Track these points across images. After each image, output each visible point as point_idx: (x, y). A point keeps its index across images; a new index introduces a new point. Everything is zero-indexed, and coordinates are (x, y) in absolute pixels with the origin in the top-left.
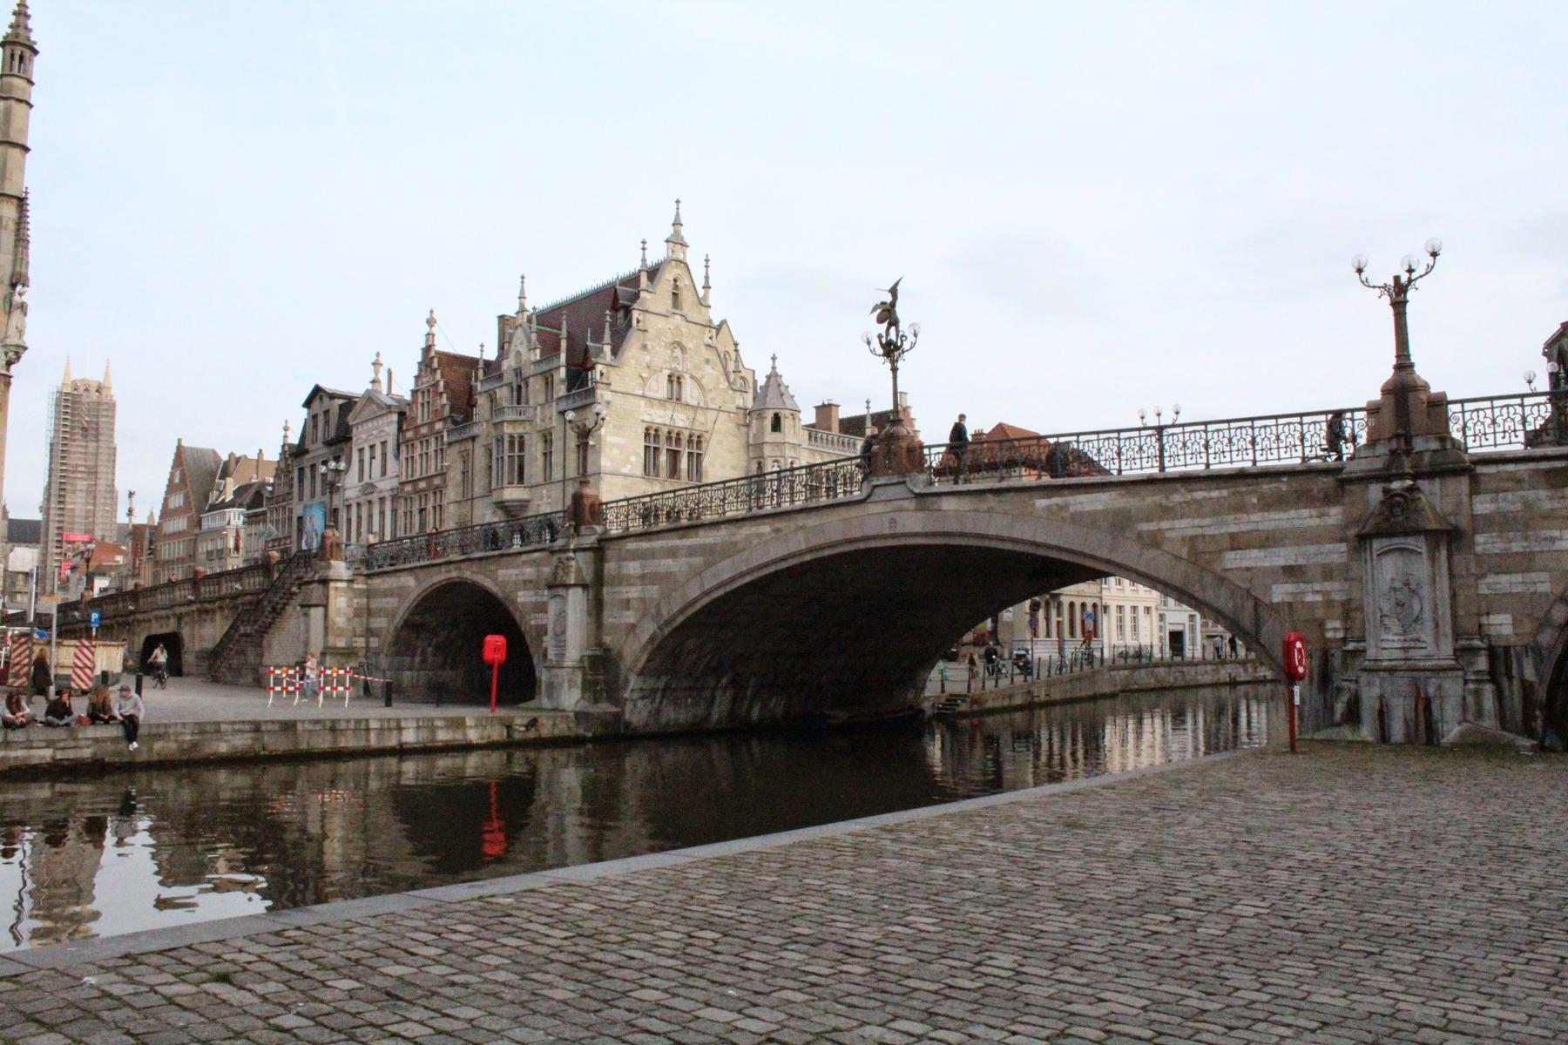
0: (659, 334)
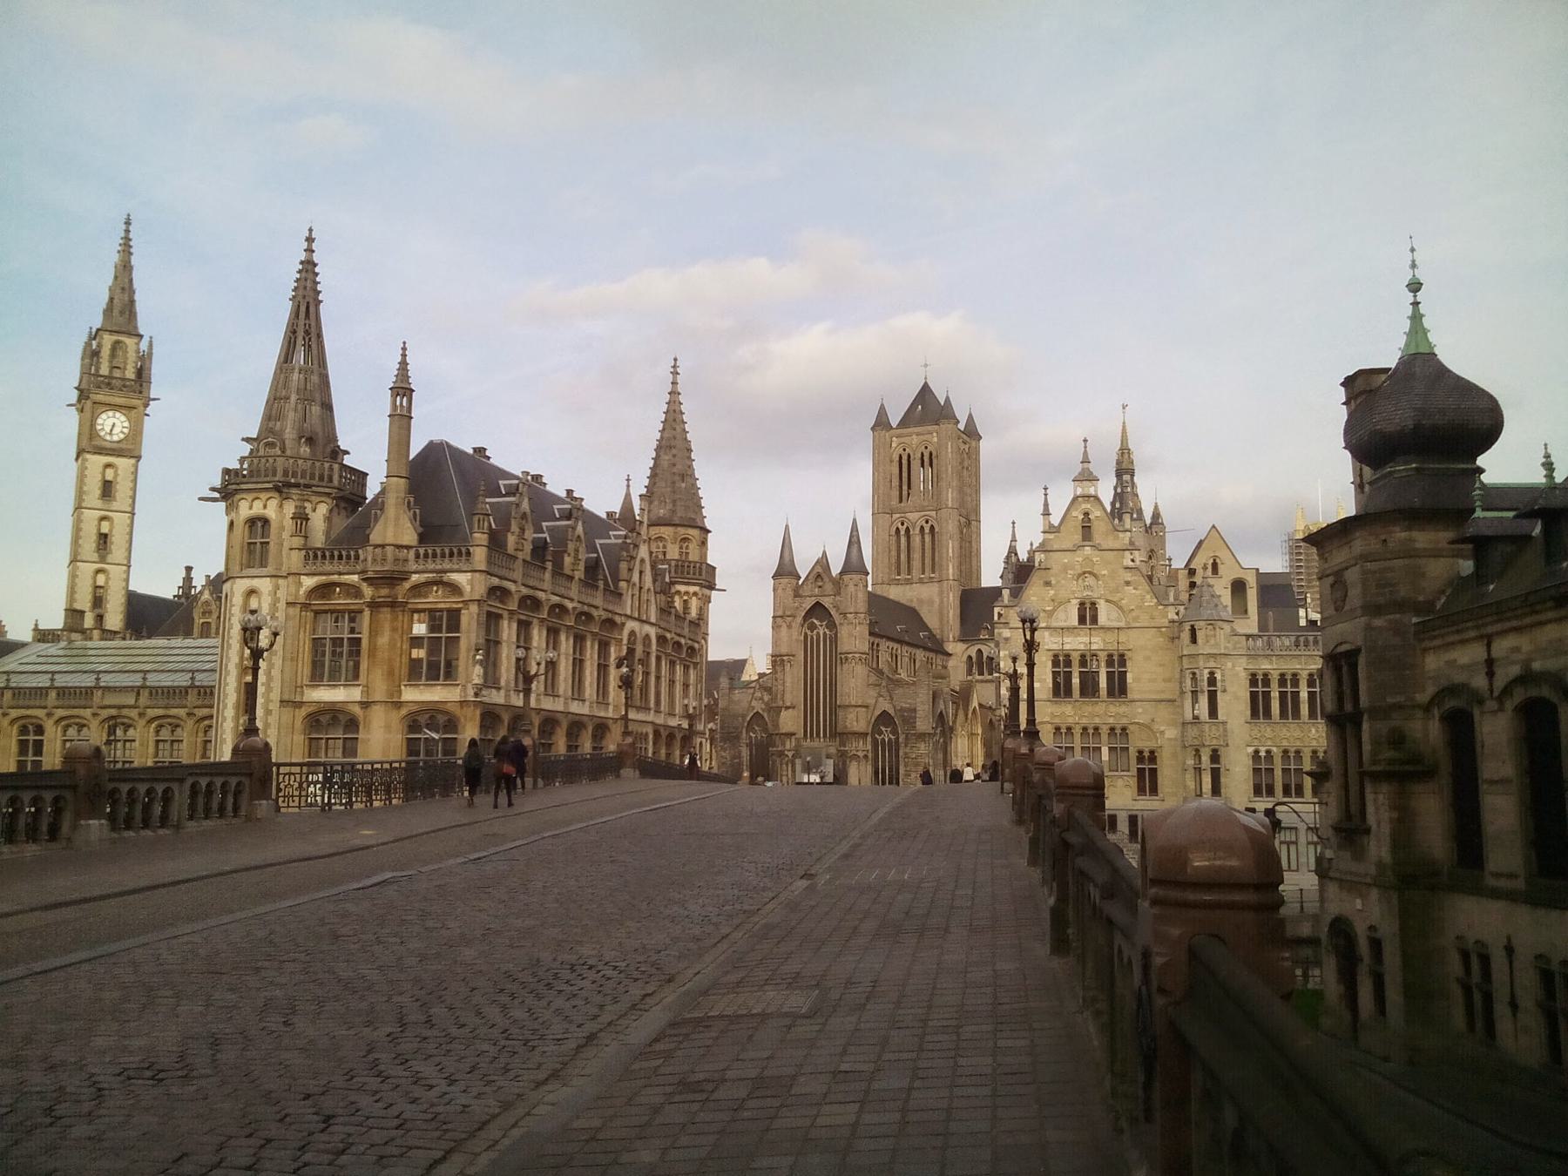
0: (1065, 568)
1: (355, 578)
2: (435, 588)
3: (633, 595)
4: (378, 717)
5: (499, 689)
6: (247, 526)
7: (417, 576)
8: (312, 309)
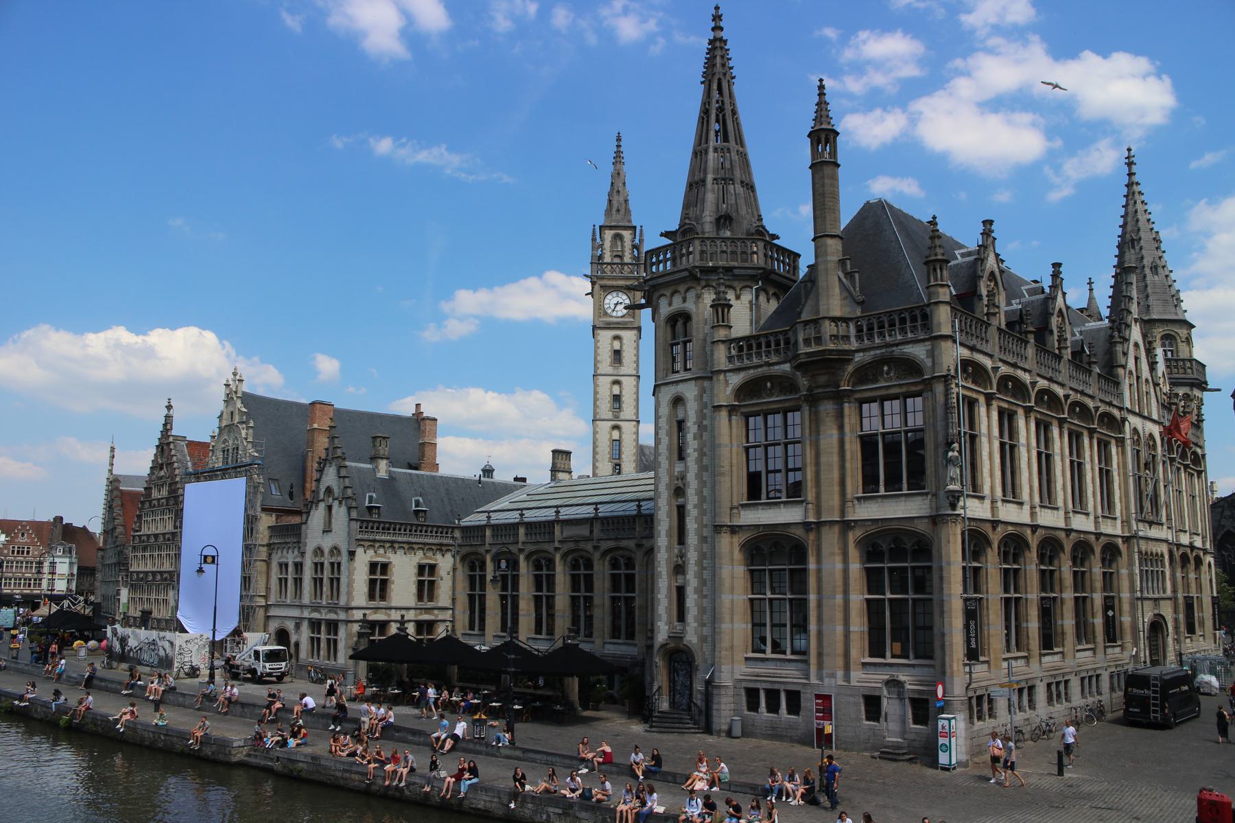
1: (787, 367)
2: (886, 368)
3: (1130, 385)
4: (831, 538)
5: (982, 498)
6: (669, 325)
7: (861, 354)
8: (725, 85)
